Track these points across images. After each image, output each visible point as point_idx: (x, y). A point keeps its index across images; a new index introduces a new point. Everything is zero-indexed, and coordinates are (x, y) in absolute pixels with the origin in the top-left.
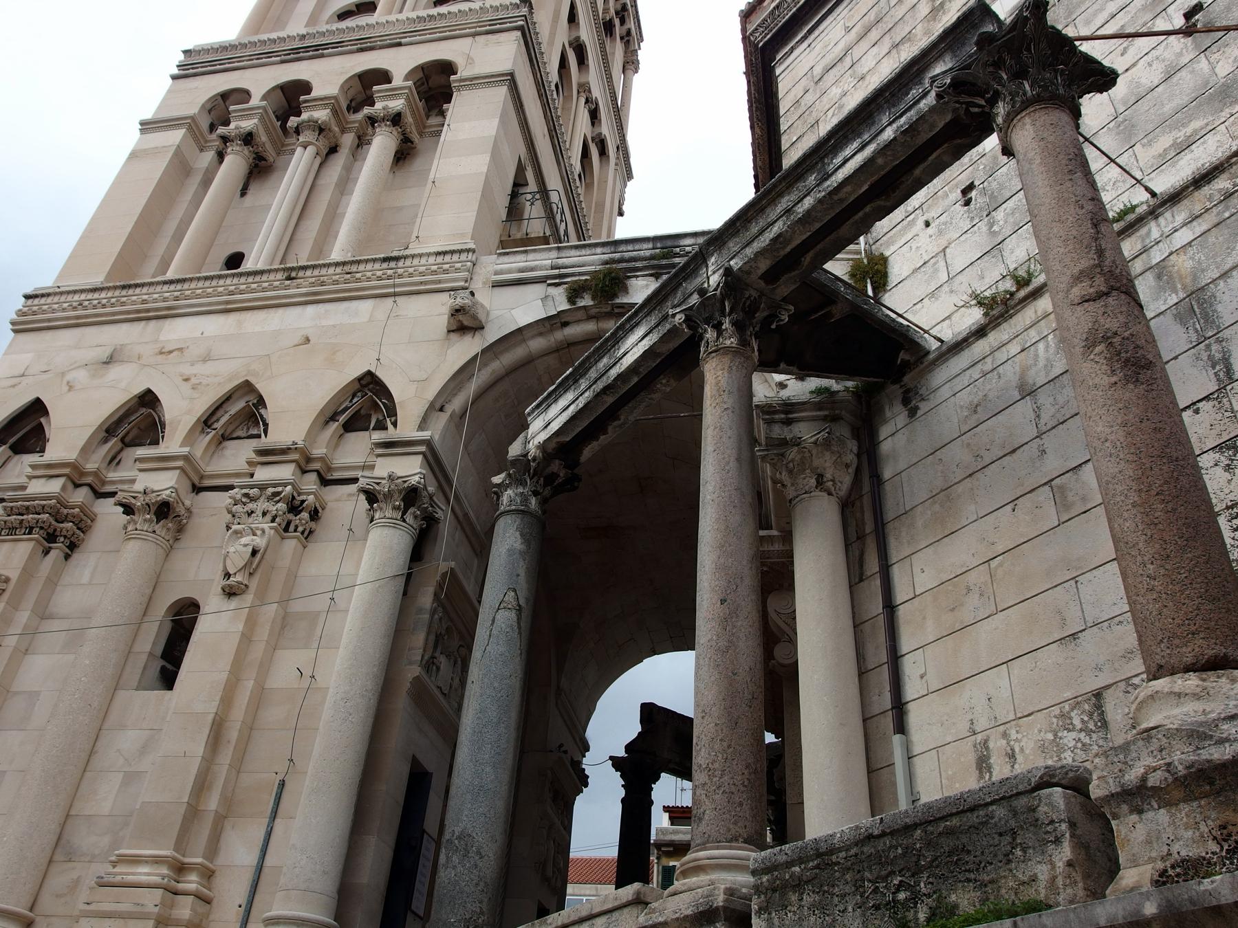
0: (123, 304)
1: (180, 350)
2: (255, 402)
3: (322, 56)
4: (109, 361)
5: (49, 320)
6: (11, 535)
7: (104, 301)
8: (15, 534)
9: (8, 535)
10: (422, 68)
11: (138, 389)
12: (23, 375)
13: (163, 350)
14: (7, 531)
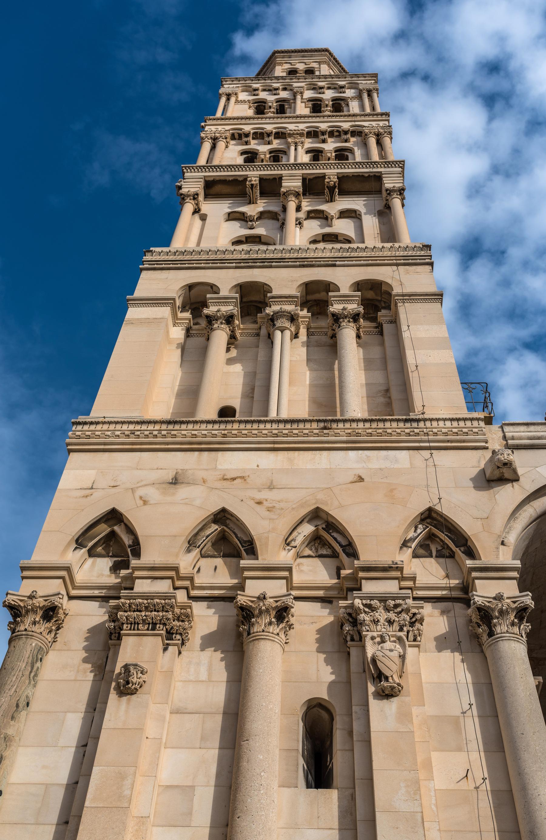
0: (175, 436)
1: (242, 478)
2: (324, 526)
3: (271, 267)
4: (175, 481)
5: (105, 444)
6: (134, 630)
7: (155, 433)
8: (138, 629)
9: (130, 629)
10: (358, 284)
11: (215, 508)
12: (92, 488)
13: (226, 477)
14: (129, 626)
